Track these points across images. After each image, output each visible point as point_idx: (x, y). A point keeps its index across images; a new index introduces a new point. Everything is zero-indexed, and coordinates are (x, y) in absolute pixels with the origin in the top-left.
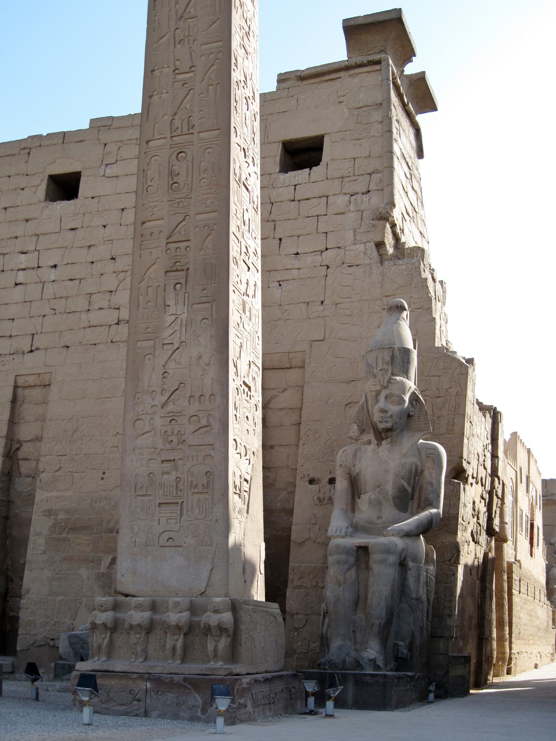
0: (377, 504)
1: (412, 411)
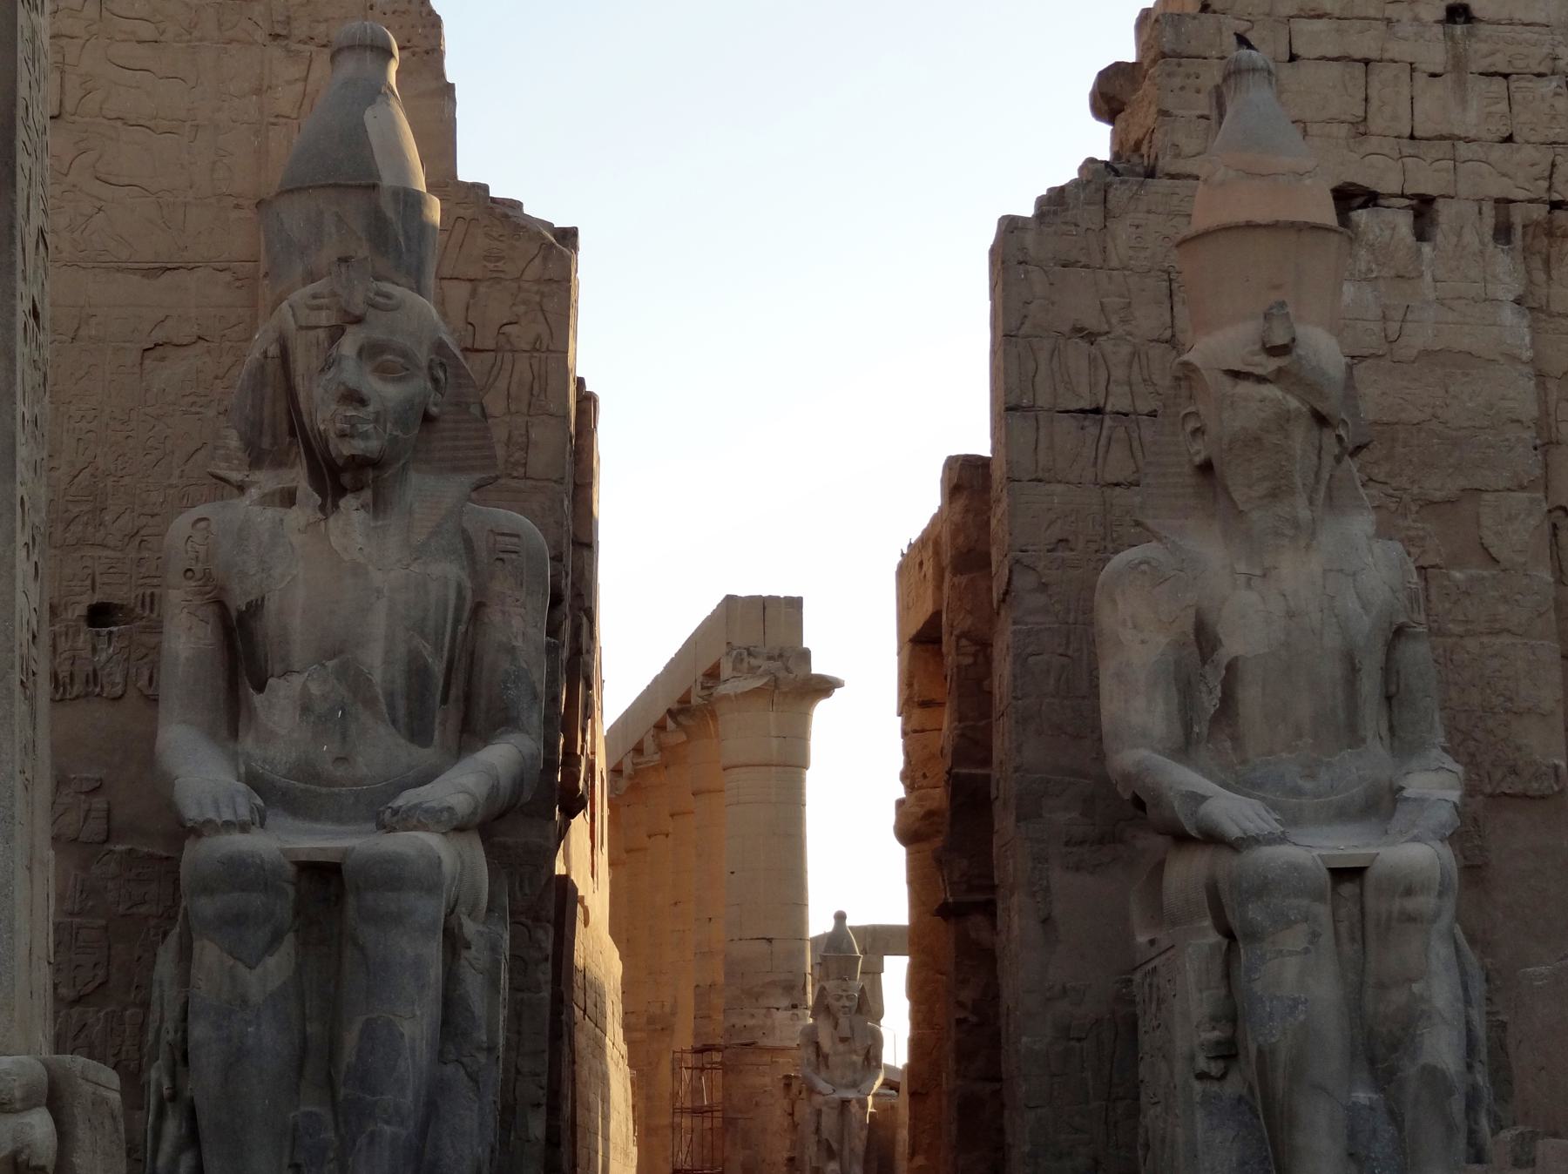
1: (436, 405)
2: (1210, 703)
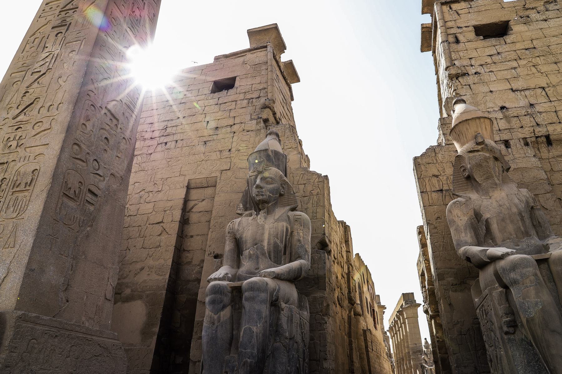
0: (255, 258)
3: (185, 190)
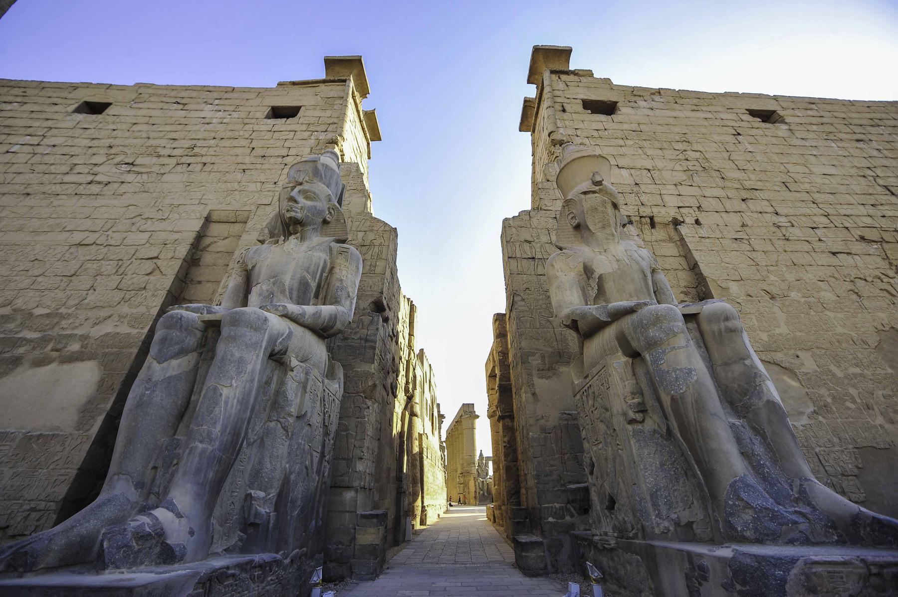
2: (593, 293)
3: (202, 221)
